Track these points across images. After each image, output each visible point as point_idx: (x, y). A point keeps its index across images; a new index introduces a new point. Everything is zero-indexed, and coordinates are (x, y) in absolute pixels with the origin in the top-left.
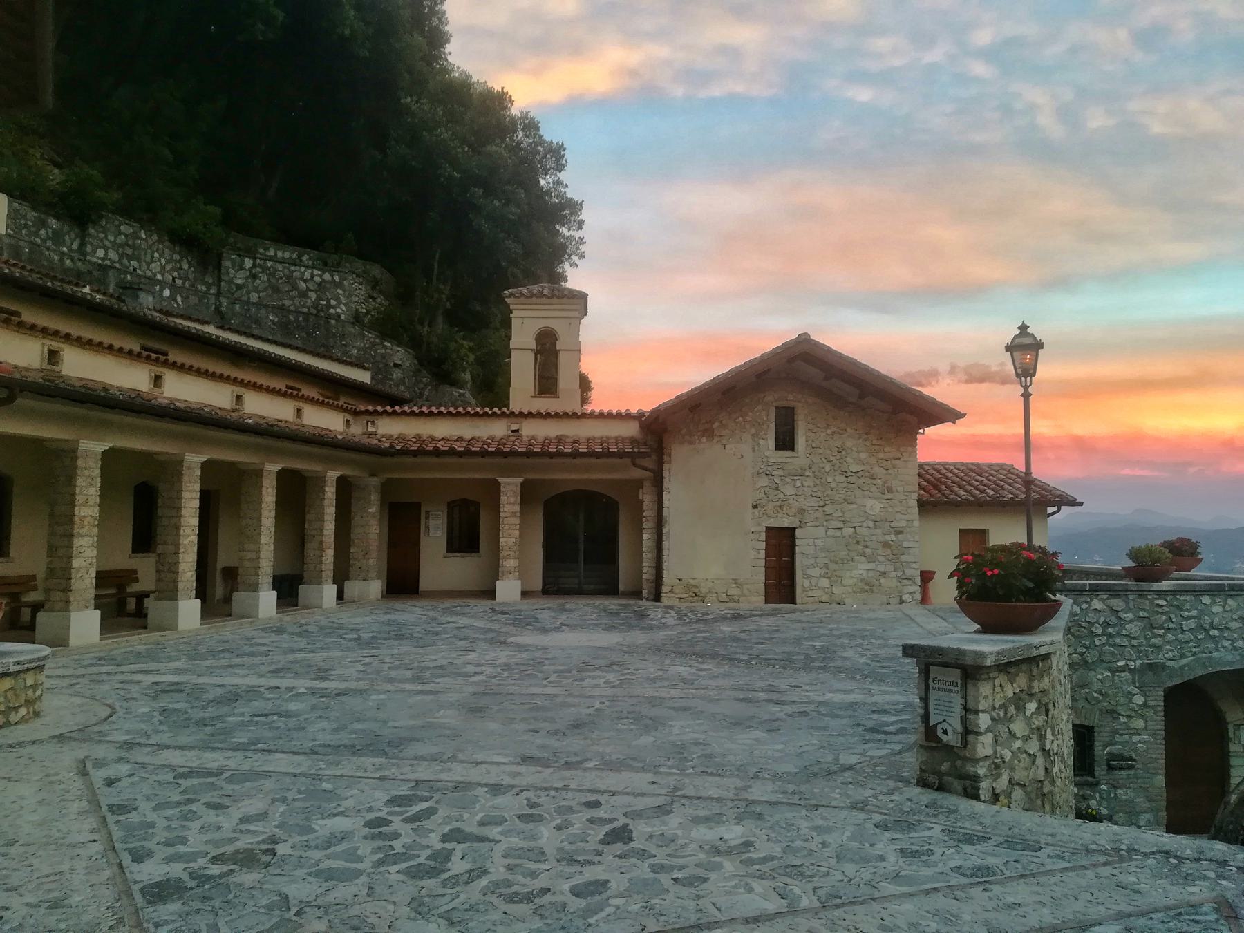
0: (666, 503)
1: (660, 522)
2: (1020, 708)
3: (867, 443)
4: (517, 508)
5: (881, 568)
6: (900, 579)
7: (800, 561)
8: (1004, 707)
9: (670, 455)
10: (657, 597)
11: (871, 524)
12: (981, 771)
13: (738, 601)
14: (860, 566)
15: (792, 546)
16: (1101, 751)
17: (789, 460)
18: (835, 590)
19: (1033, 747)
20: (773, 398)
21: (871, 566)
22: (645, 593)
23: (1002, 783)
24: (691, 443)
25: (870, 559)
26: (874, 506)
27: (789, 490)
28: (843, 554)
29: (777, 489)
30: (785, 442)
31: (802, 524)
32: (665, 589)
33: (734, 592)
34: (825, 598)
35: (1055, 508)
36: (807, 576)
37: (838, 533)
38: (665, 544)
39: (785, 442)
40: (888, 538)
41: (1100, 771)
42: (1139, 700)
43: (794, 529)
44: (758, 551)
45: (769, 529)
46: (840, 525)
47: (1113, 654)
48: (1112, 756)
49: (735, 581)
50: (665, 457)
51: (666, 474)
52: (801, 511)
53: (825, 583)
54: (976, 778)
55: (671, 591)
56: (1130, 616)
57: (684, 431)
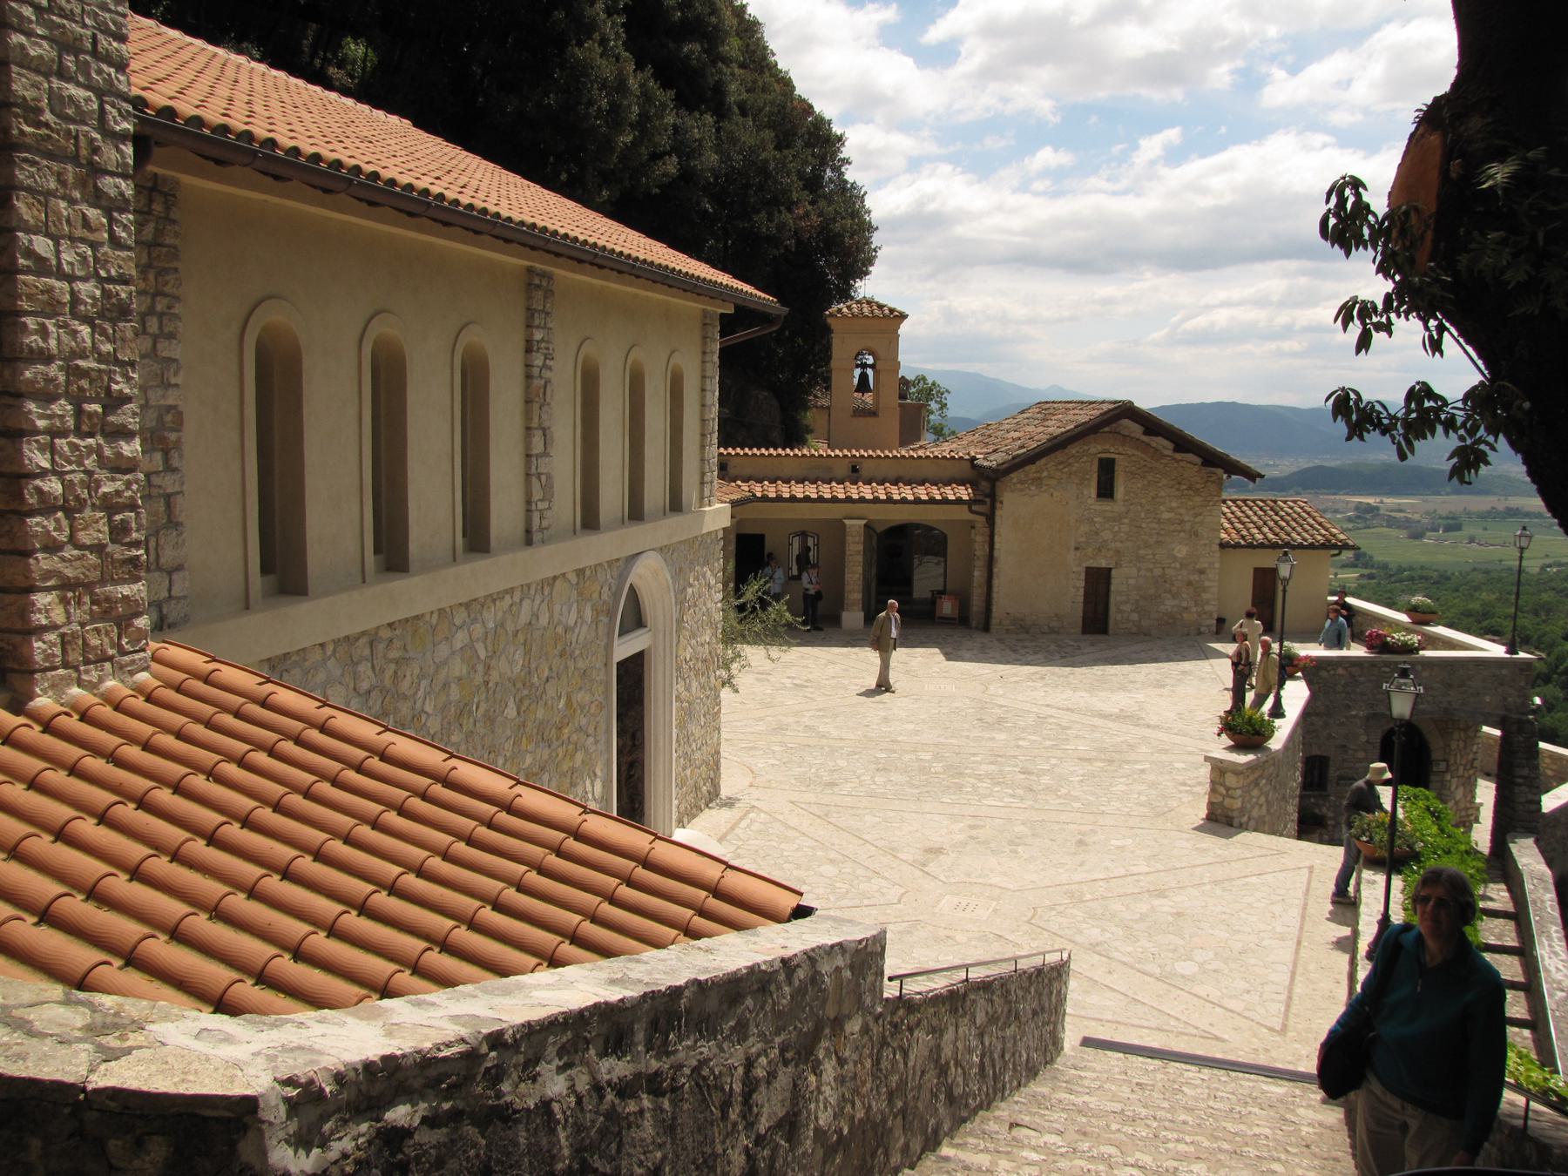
0: (997, 546)
1: (991, 560)
2: (1257, 785)
3: (1177, 493)
4: (861, 547)
5: (1184, 604)
6: (1199, 615)
7: (1113, 599)
8: (1249, 785)
9: (1001, 502)
10: (986, 628)
11: (1178, 566)
12: (1235, 814)
13: (1058, 633)
14: (1167, 602)
15: (1108, 583)
16: (1333, 773)
17: (1108, 508)
18: (1143, 623)
19: (1262, 799)
20: (1097, 448)
21: (1176, 602)
22: (974, 623)
23: (1245, 819)
24: (1022, 490)
25: (1175, 596)
26: (1181, 551)
27: (1107, 535)
28: (1152, 591)
29: (1097, 534)
30: (1106, 491)
31: (1118, 565)
32: (994, 621)
33: (1054, 624)
34: (1134, 630)
35: (1336, 552)
36: (1119, 611)
37: (1149, 574)
38: (996, 582)
39: (1106, 491)
40: (1192, 577)
41: (1331, 788)
42: (1364, 738)
43: (1110, 569)
44: (1078, 589)
45: (1088, 569)
46: (1151, 566)
47: (1349, 707)
48: (1341, 778)
49: (1056, 615)
50: (998, 505)
51: (998, 520)
52: (1118, 552)
53: (1135, 616)
54: (1232, 818)
55: (1000, 624)
56: (1362, 679)
57: (1015, 480)
